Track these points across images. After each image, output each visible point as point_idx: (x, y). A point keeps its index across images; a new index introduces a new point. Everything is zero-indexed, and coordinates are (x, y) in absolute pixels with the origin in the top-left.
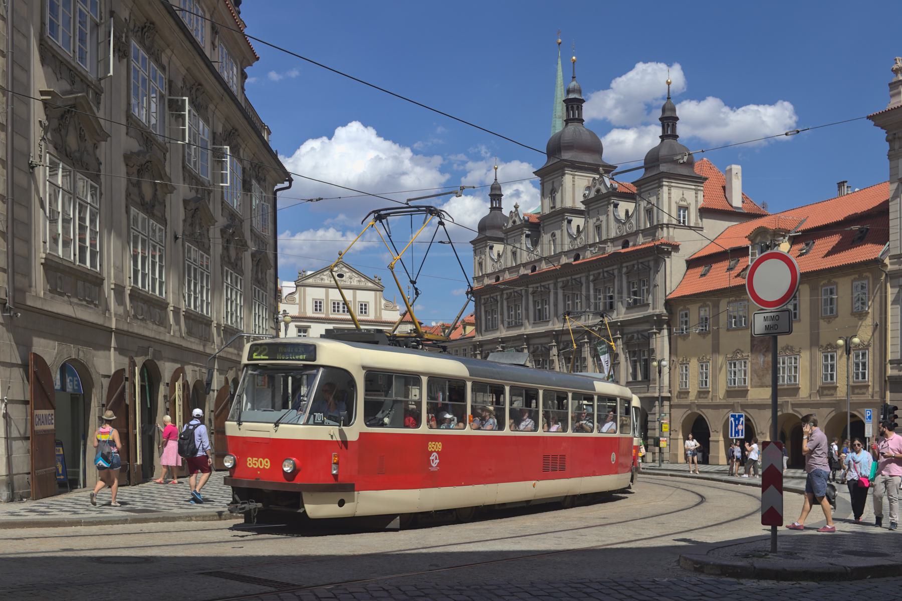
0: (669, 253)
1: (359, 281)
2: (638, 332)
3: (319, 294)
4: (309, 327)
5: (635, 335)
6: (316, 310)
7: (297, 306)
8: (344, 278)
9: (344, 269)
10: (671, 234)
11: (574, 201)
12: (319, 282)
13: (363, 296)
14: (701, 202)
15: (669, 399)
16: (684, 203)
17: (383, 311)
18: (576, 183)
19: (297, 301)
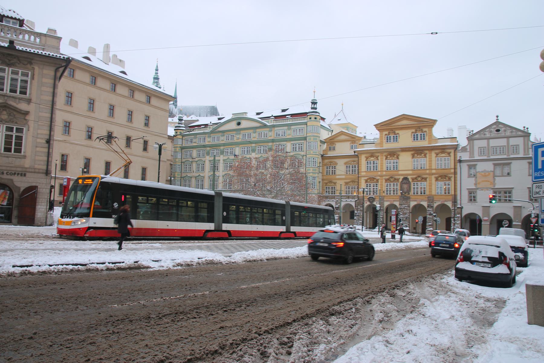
1: (512, 132)
3: (483, 143)
4: (476, 165)
7: (468, 153)
9: (500, 126)
12: (483, 136)
13: (513, 141)
19: (468, 150)
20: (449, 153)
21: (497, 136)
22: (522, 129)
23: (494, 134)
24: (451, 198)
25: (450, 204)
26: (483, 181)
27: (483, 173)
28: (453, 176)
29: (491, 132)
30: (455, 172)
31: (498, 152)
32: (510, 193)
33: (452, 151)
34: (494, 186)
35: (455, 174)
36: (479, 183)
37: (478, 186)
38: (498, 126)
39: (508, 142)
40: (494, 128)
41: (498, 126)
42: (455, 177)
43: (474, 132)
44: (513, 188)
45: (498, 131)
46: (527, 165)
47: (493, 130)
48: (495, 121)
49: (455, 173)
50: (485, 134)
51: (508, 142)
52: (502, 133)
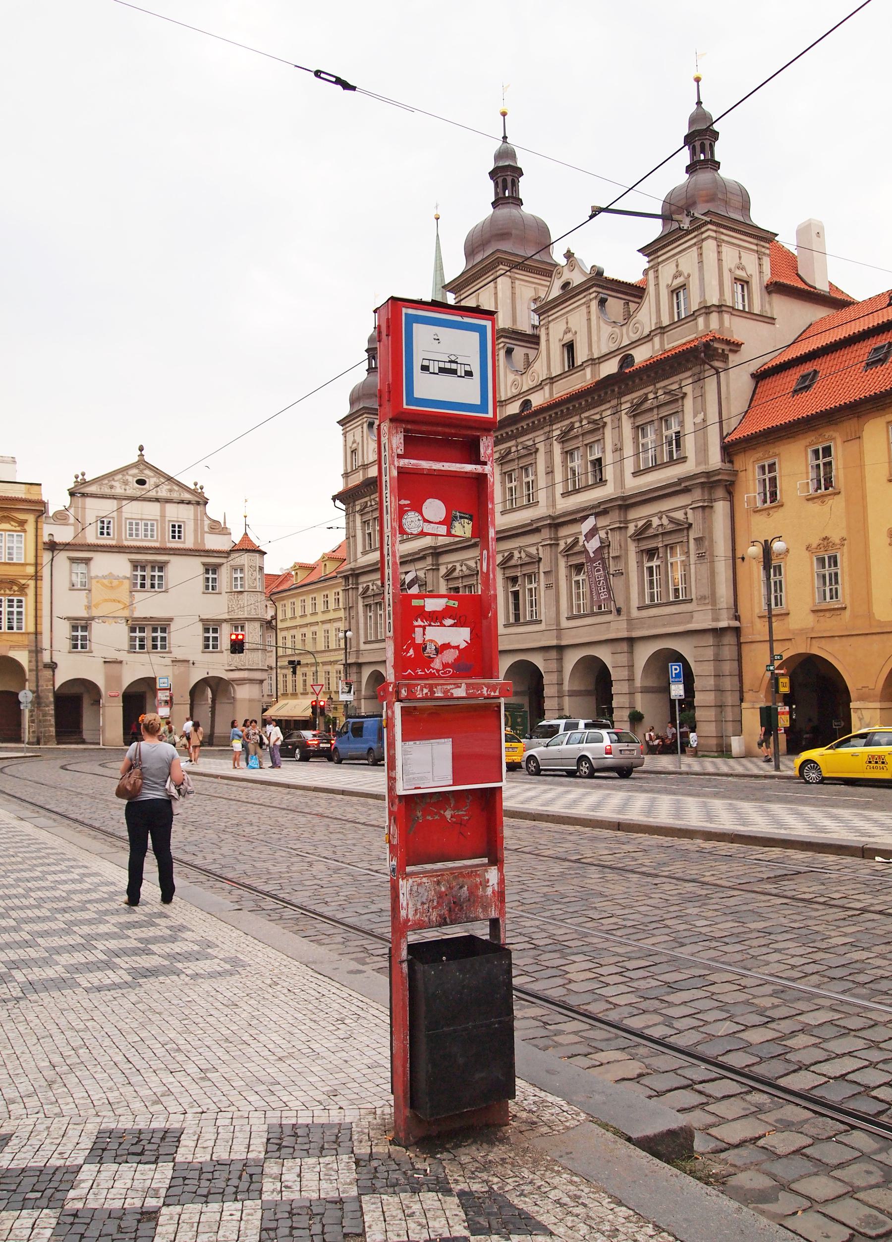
0: (725, 358)
1: (170, 491)
2: (660, 515)
4: (90, 559)
5: (655, 522)
6: (102, 533)
7: (72, 528)
8: (146, 486)
9: (147, 472)
10: (727, 324)
11: (514, 320)
12: (106, 491)
13: (175, 513)
14: (767, 277)
15: (737, 631)
16: (741, 274)
17: (206, 535)
18: (517, 291)
20: (22, 523)
21: (138, 494)
22: (193, 487)
23: (134, 489)
24: (25, 640)
25: (22, 657)
26: (106, 601)
27: (106, 581)
28: (32, 583)
29: (126, 483)
30: (36, 572)
31: (142, 532)
32: (164, 630)
33: (31, 518)
34: (132, 611)
35: (36, 580)
36: (96, 606)
37: (95, 613)
38: (141, 471)
39: (163, 511)
40: (134, 476)
41: (141, 471)
42: (36, 587)
43: (88, 478)
44: (171, 620)
45: (141, 482)
46: (201, 570)
47: (130, 479)
48: (136, 459)
49: (37, 577)
50: (112, 487)
51: (163, 511)
52: (149, 489)
